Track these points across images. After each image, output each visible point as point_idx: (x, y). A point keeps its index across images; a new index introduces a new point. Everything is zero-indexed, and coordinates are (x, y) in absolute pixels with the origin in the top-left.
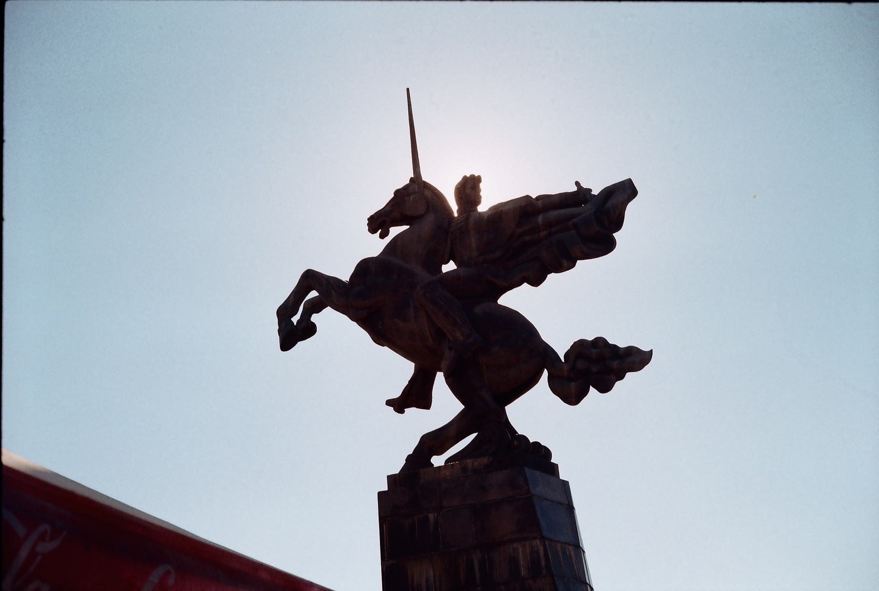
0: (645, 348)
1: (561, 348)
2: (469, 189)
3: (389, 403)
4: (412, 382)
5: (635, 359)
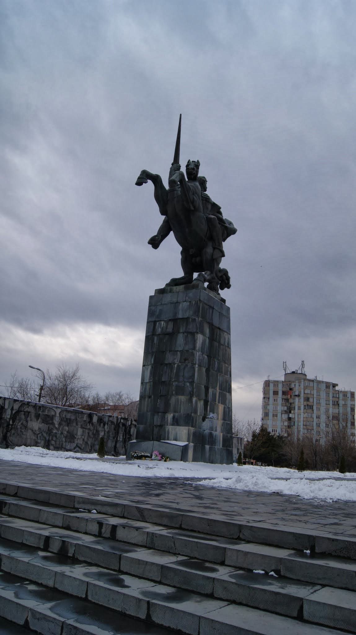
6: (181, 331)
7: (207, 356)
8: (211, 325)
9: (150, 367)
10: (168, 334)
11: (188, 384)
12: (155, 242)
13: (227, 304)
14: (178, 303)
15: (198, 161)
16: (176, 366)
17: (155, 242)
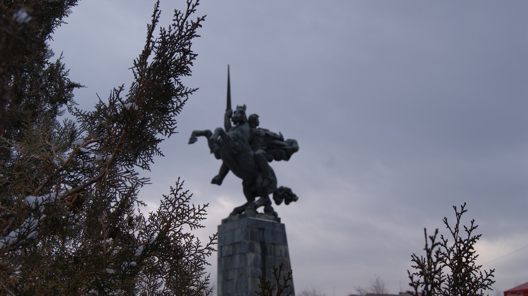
6: (238, 252)
7: (262, 269)
8: (263, 244)
9: (220, 283)
10: (230, 256)
11: (244, 294)
12: (218, 181)
14: (234, 230)
16: (235, 281)
17: (218, 181)
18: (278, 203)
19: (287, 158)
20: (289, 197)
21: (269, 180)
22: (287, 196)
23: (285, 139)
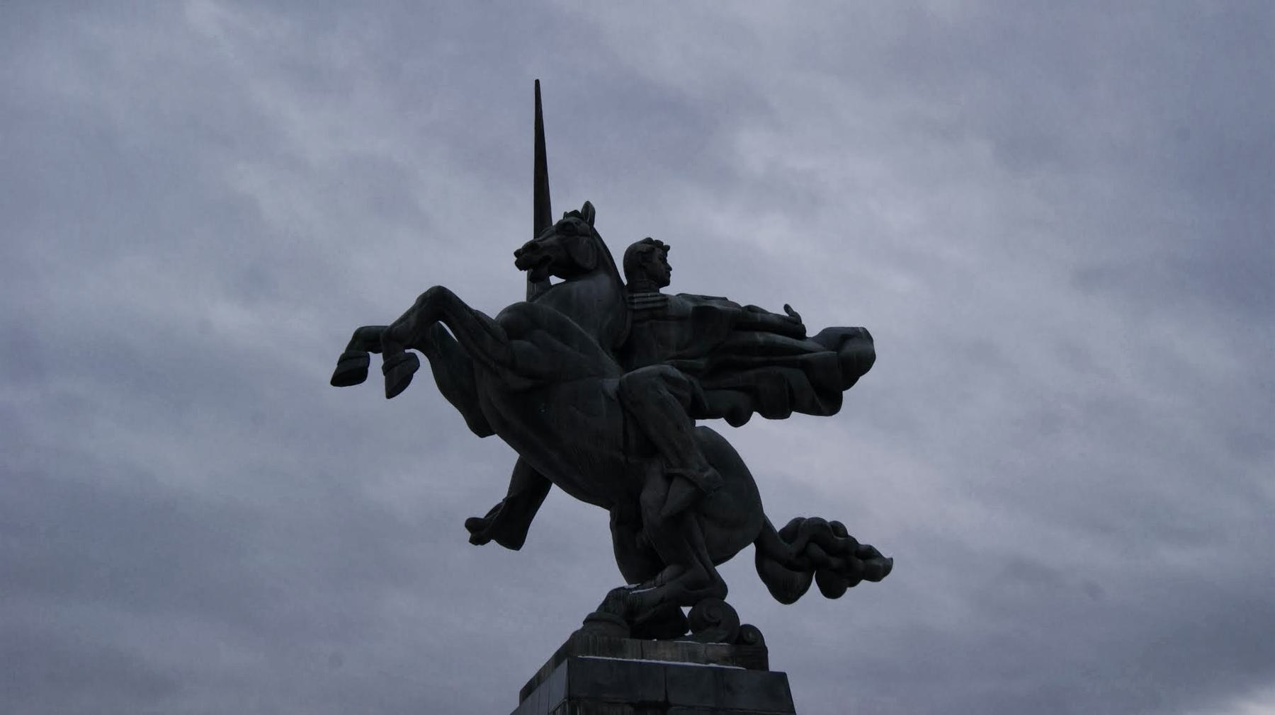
0: (886, 554)
1: (779, 524)
2: (650, 260)
3: (472, 524)
4: (508, 501)
5: (869, 565)
12: (506, 525)
13: (774, 665)
15: (588, 207)
17: (506, 525)
18: (786, 592)
19: (826, 401)
20: (835, 562)
21: (691, 482)
22: (824, 558)
23: (813, 329)
